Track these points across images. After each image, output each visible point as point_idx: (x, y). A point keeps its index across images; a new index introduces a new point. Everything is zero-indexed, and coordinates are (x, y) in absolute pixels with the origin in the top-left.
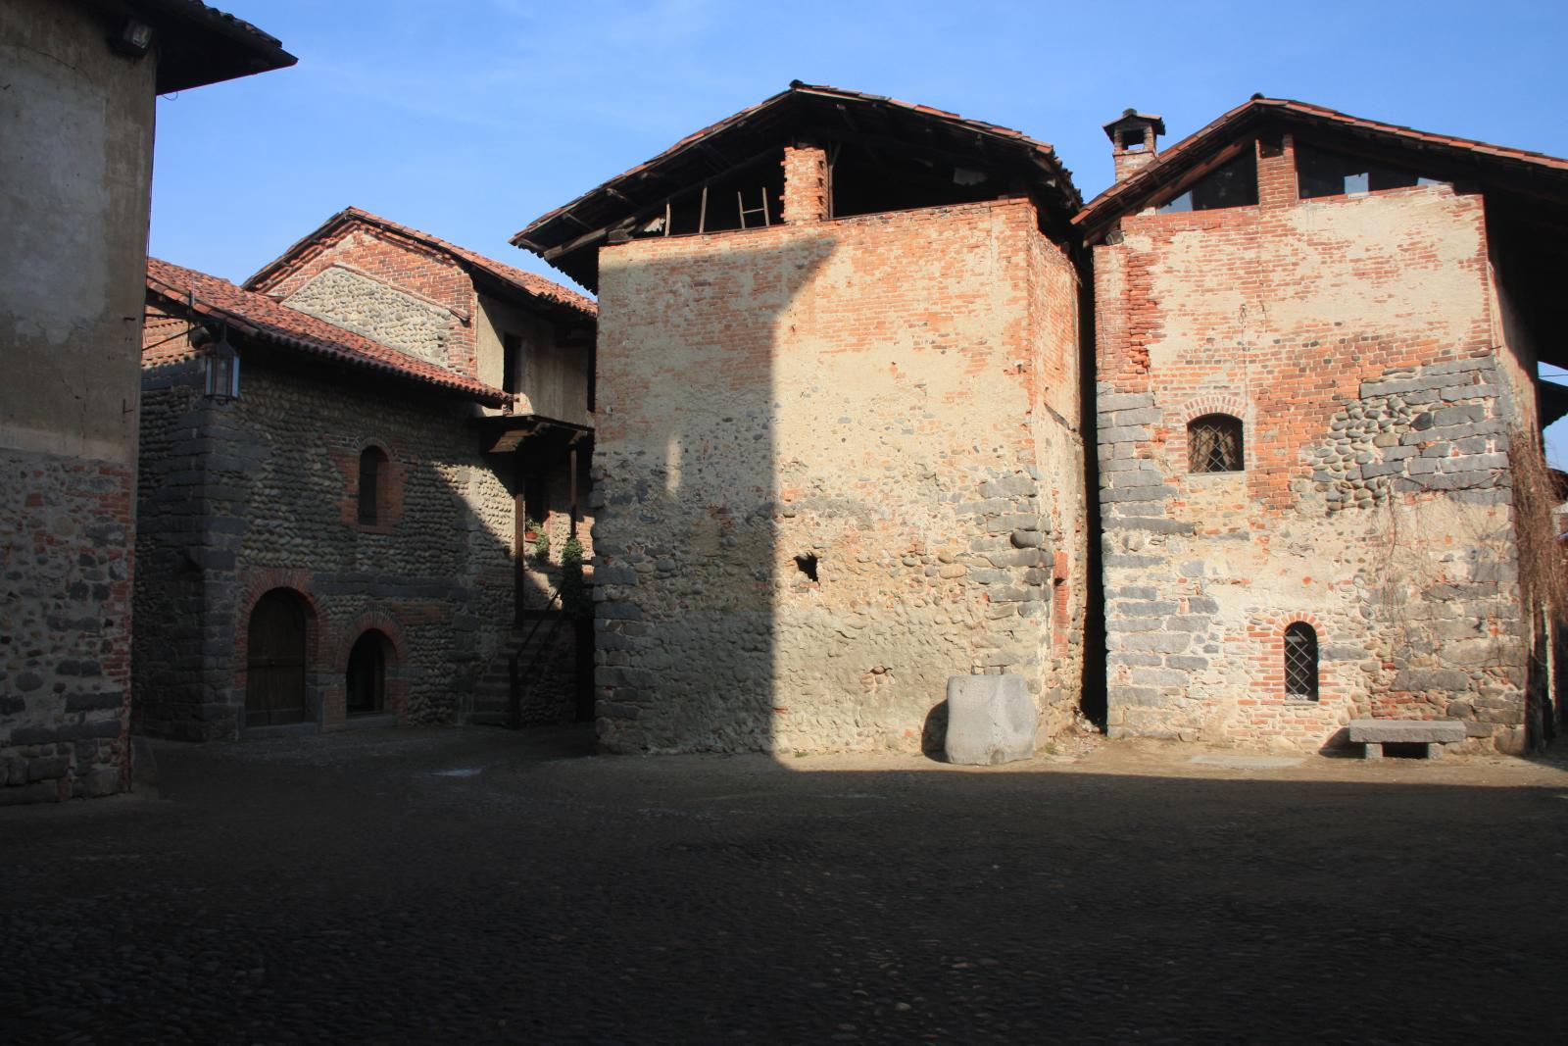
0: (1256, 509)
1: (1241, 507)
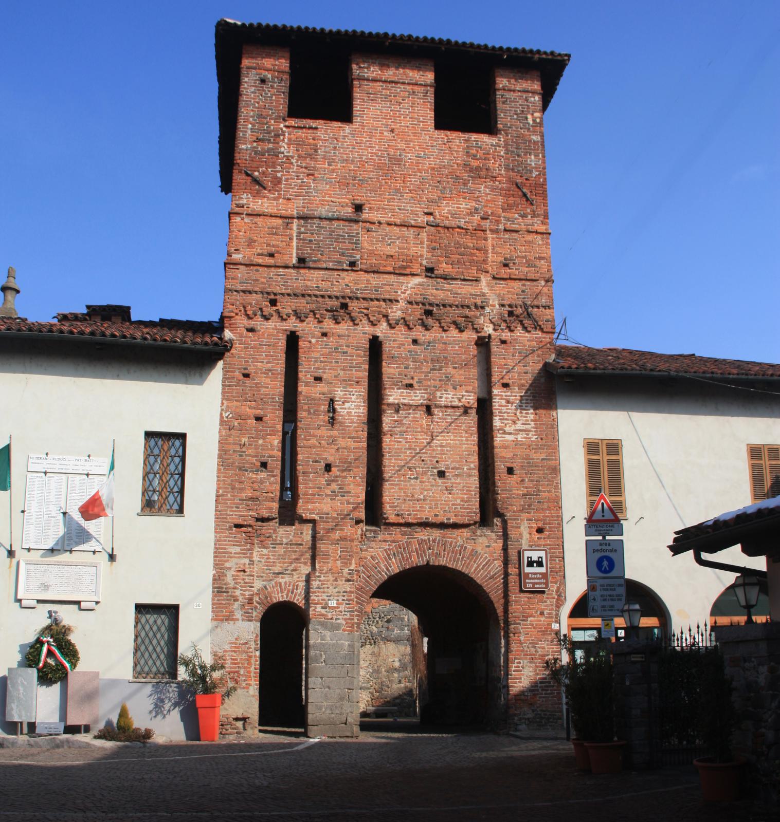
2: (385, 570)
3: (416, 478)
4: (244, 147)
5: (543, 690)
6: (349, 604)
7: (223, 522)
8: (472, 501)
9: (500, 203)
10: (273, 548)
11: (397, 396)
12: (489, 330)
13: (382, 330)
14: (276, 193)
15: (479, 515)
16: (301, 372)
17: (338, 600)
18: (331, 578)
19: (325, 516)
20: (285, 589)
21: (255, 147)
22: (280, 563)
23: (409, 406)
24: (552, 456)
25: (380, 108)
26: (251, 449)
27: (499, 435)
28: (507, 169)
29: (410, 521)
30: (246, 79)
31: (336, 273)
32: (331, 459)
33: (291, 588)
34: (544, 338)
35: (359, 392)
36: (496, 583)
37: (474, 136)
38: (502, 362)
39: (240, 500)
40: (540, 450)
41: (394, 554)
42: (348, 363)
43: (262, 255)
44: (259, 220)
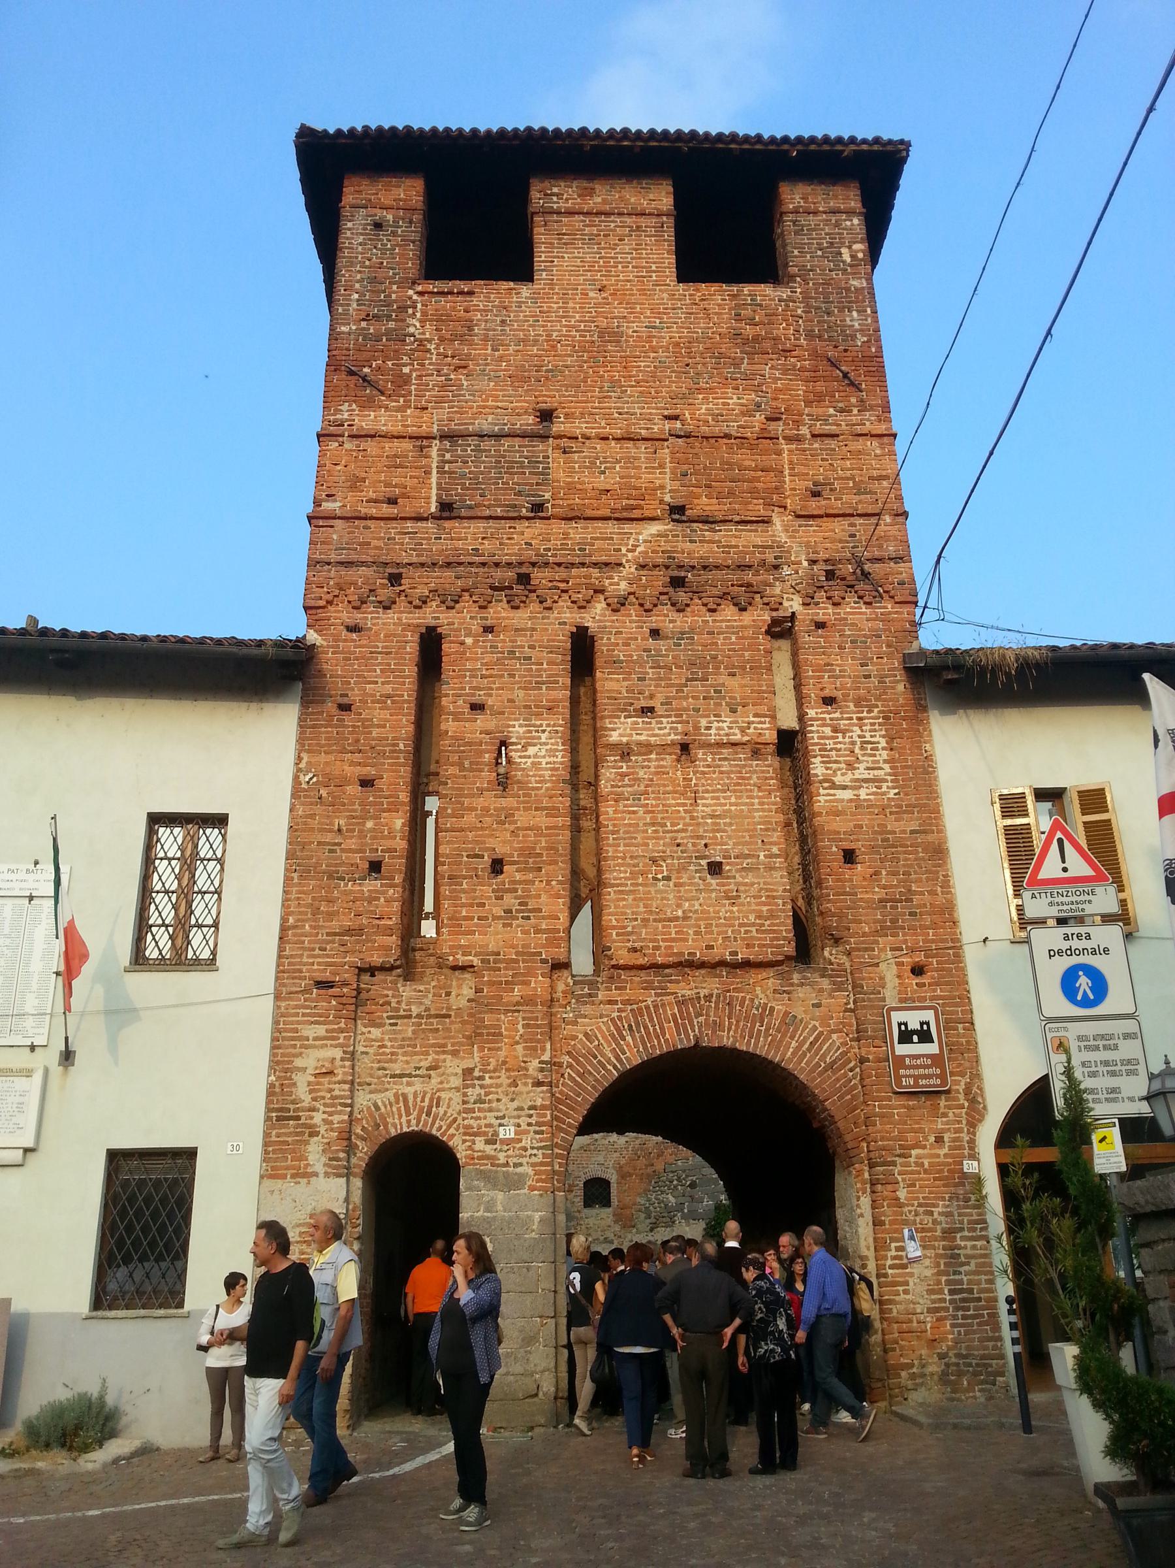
0: (617, 1228)
1: (609, 1226)
2: (613, 1059)
3: (668, 878)
4: (344, 329)
5: (957, 1309)
6: (542, 1132)
7: (293, 978)
8: (778, 917)
9: (801, 392)
10: (391, 1024)
11: (625, 729)
12: (794, 604)
13: (596, 616)
14: (402, 400)
15: (793, 944)
16: (447, 695)
17: (519, 1126)
18: (504, 1080)
19: (491, 958)
20: (415, 1106)
21: (364, 329)
22: (405, 1054)
23: (647, 748)
24: (931, 824)
25: (581, 255)
26: (351, 838)
27: (822, 791)
28: (810, 335)
29: (660, 960)
30: (350, 225)
31: (508, 524)
32: (501, 850)
33: (426, 1104)
34: (896, 613)
35: (554, 725)
36: (838, 1080)
37: (747, 289)
38: (822, 660)
39: (328, 934)
40: (905, 816)
41: (630, 1026)
42: (531, 676)
43: (376, 501)
44: (371, 446)
